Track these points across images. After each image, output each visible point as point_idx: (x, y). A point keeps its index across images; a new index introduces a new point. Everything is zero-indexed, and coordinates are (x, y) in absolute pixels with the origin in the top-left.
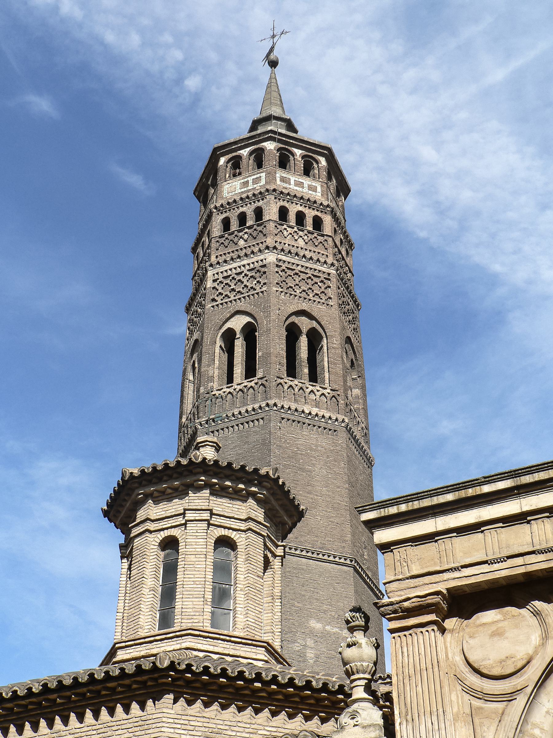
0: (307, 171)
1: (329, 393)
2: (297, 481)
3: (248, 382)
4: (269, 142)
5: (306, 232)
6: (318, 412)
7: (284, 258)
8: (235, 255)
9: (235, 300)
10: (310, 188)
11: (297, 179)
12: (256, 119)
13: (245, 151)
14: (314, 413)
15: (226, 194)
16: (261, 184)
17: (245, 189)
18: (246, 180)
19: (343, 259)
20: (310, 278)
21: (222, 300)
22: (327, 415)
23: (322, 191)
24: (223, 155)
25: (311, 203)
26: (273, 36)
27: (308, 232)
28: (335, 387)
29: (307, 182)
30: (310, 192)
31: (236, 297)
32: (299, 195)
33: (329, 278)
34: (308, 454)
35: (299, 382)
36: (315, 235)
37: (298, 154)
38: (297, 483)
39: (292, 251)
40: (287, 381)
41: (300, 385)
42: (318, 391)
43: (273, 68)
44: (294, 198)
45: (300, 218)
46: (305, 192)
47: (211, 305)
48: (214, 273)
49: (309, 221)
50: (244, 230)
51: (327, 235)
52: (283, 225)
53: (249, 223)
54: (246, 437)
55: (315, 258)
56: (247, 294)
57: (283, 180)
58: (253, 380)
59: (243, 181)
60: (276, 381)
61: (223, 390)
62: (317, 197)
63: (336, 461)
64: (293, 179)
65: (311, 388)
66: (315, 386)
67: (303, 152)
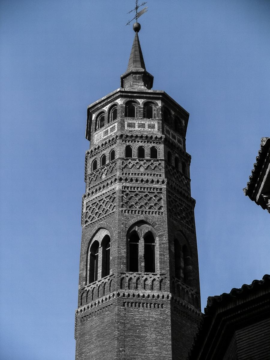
0: (148, 114)
1: (158, 278)
2: (134, 345)
3: (104, 279)
4: (120, 99)
5: (145, 161)
6: (150, 294)
7: (128, 185)
8: (97, 187)
9: (98, 220)
10: (150, 126)
11: (140, 122)
12: (122, 76)
13: (106, 108)
14: (146, 295)
15: (96, 142)
16: (115, 131)
17: (106, 136)
18: (107, 129)
19: (178, 172)
20: (147, 195)
21: (91, 221)
22: (156, 295)
23: (159, 127)
24: (94, 112)
25: (148, 139)
26: (137, 8)
27: (146, 161)
28: (163, 271)
29: (147, 122)
30: (149, 130)
31: (99, 218)
32: (139, 135)
33: (161, 192)
34: (142, 325)
35: (137, 274)
36: (152, 161)
37: (141, 103)
38: (135, 347)
39: (133, 179)
40: (127, 275)
41: (138, 276)
42: (151, 277)
43: (137, 32)
44: (134, 138)
45: (141, 151)
46: (147, 131)
47: (85, 225)
48: (87, 201)
49: (147, 151)
50: (104, 167)
51: (161, 160)
52: (128, 160)
53: (107, 162)
54: (103, 319)
55: (150, 180)
56: (105, 215)
57: (130, 125)
58: (107, 278)
59: (105, 130)
60: (120, 276)
61: (91, 287)
62: (154, 132)
63: (163, 326)
64: (137, 122)
65: (145, 277)
66: (149, 274)
67: (145, 100)
